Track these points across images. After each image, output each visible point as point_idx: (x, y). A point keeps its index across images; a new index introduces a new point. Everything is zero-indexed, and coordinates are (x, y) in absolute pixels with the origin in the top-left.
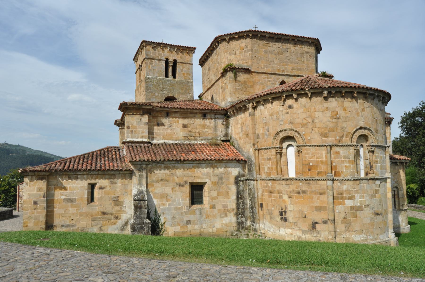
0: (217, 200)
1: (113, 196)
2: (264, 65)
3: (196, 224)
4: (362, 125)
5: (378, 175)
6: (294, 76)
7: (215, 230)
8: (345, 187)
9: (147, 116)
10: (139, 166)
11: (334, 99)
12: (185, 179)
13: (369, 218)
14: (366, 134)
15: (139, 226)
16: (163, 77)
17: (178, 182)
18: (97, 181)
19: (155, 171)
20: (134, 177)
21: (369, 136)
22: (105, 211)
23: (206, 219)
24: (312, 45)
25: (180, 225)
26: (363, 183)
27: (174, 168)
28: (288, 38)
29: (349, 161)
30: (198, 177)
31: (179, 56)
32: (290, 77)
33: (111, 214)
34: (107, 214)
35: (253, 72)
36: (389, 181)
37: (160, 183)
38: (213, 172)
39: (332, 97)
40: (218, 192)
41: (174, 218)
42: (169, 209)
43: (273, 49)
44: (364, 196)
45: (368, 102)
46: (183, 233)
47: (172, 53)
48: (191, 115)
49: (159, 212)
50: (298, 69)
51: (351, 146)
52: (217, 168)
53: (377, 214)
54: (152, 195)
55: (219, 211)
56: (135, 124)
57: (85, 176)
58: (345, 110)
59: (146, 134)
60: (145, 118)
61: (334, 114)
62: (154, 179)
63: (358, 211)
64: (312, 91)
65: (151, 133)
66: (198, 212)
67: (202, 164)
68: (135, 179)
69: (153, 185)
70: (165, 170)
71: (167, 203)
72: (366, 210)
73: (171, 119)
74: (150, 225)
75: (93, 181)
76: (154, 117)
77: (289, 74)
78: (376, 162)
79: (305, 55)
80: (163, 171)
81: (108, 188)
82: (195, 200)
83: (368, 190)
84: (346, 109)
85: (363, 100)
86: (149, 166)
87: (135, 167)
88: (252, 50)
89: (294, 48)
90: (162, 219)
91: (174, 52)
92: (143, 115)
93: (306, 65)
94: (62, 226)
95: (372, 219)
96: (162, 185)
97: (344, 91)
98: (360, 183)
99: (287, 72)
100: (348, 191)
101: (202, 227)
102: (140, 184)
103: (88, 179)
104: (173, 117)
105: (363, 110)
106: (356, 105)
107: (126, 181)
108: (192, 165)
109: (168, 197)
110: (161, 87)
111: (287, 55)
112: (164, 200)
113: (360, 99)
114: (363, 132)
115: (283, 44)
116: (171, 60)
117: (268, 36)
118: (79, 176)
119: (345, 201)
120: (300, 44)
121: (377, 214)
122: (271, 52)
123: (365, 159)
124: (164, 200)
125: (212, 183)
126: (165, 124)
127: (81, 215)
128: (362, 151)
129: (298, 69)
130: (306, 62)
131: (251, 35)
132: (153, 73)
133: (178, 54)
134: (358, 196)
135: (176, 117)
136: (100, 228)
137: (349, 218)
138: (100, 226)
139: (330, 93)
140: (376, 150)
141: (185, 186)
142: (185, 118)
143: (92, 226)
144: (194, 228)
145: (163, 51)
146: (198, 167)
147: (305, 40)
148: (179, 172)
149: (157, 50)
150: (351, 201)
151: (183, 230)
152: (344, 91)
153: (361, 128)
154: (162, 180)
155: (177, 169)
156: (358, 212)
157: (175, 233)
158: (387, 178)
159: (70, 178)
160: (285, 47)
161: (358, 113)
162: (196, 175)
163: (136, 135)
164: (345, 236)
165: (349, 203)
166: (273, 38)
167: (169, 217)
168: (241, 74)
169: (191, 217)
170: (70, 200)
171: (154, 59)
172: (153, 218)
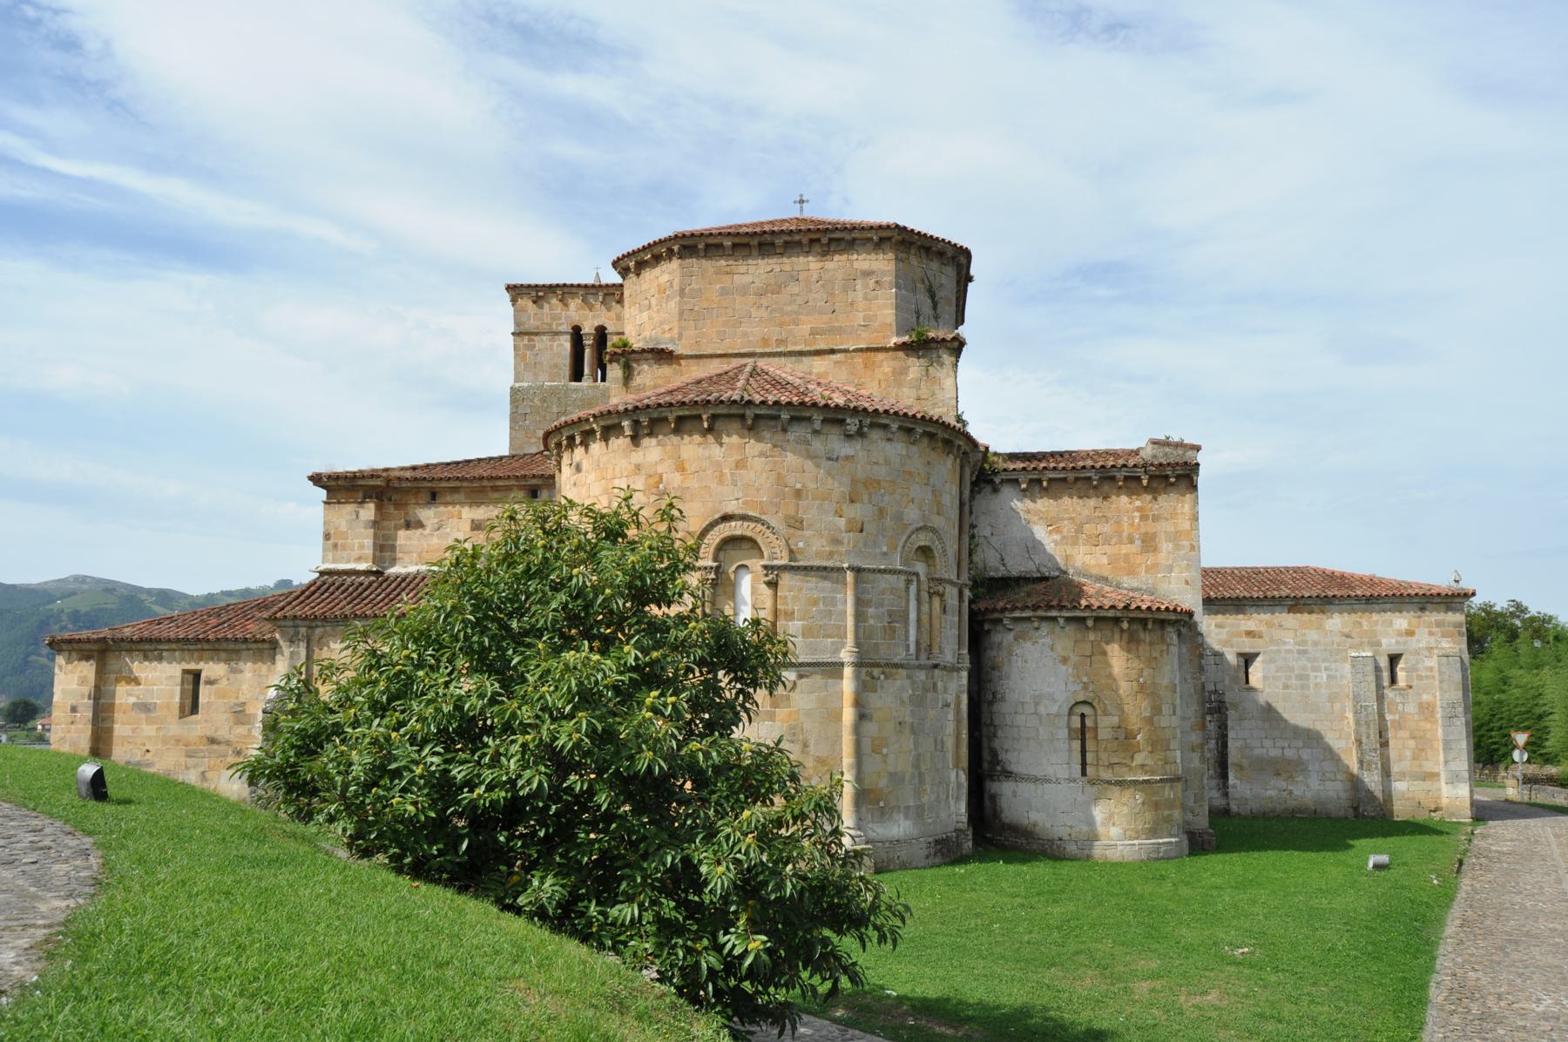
2: (718, 333)
4: (732, 507)
6: (818, 353)
9: (372, 506)
10: (291, 631)
11: (654, 441)
14: (749, 534)
16: (563, 380)
18: (201, 666)
20: (278, 657)
24: (886, 246)
28: (797, 238)
31: (612, 314)
32: (805, 359)
33: (228, 743)
34: (219, 743)
35: (681, 357)
36: (848, 671)
39: (650, 435)
43: (748, 279)
45: (759, 440)
47: (591, 308)
48: (496, 495)
50: (831, 331)
56: (343, 526)
58: (683, 470)
59: (369, 551)
60: (369, 511)
61: (652, 481)
64: (602, 423)
65: (384, 549)
73: (442, 509)
75: (192, 666)
76: (398, 505)
77: (798, 348)
78: (790, 615)
79: (858, 281)
81: (224, 682)
84: (687, 466)
85: (742, 437)
86: (318, 631)
87: (282, 635)
88: (682, 292)
89: (820, 265)
91: (598, 305)
92: (363, 502)
93: (861, 315)
97: (671, 417)
99: (795, 344)
104: (446, 504)
105: (740, 464)
106: (716, 451)
107: (263, 668)
110: (555, 410)
111: (796, 290)
113: (729, 435)
114: (735, 528)
115: (785, 260)
116: (588, 329)
117: (728, 243)
120: (840, 252)
122: (744, 290)
127: (165, 741)
129: (831, 331)
130: (861, 304)
131: (676, 248)
132: (535, 374)
133: (609, 310)
135: (453, 504)
139: (636, 424)
140: (786, 580)
142: (479, 504)
143: (187, 768)
145: (566, 305)
147: (856, 234)
149: (546, 306)
152: (671, 417)
153: (726, 518)
158: (842, 664)
159: (146, 658)
160: (787, 268)
161: (722, 475)
163: (345, 554)
166: (747, 245)
168: (646, 367)
170: (145, 708)
171: (537, 334)
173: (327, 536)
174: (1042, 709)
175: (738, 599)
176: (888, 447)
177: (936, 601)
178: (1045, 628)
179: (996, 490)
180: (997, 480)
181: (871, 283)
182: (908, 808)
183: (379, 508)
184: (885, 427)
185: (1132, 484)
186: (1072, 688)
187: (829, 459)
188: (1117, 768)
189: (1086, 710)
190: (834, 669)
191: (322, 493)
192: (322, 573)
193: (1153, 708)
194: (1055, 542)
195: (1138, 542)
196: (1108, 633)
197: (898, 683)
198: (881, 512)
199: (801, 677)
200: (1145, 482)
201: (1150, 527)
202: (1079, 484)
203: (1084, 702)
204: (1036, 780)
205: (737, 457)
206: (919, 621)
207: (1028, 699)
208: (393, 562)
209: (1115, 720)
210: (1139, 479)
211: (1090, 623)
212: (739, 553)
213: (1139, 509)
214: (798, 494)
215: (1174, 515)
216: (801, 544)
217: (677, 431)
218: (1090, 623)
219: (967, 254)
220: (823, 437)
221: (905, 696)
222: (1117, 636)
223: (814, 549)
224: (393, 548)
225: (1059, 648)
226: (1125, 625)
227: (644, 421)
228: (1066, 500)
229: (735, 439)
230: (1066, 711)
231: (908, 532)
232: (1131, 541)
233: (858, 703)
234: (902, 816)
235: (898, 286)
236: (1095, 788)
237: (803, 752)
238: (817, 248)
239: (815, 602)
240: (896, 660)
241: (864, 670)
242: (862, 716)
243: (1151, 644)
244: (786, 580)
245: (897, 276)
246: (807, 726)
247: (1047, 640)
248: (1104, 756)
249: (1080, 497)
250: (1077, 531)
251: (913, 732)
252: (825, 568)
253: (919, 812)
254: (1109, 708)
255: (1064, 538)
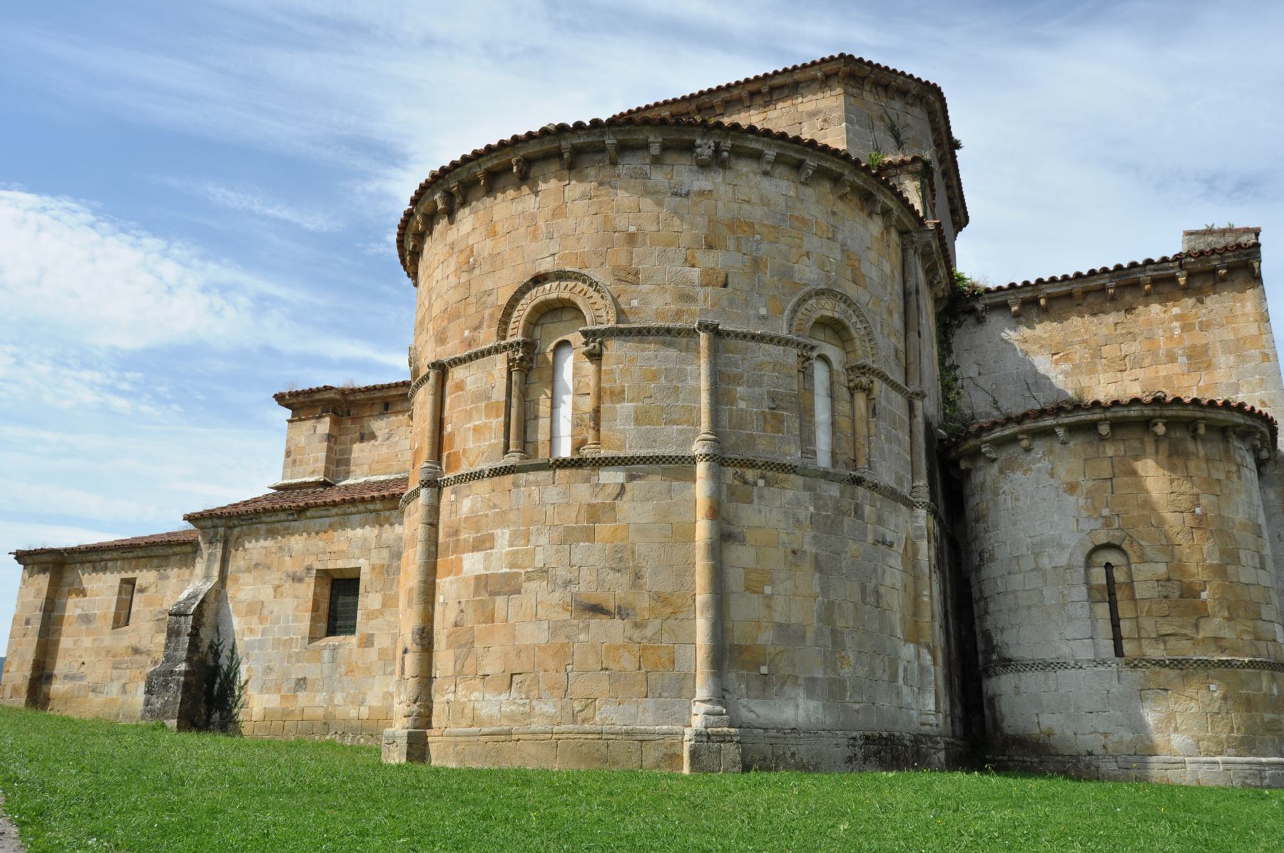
0: (380, 620)
1: (158, 608)
3: (318, 691)
4: (546, 266)
5: (622, 447)
7: (364, 713)
8: (466, 505)
9: (327, 420)
11: (467, 210)
12: (307, 563)
13: (545, 625)
14: (566, 295)
15: (162, 678)
17: (290, 570)
18: (137, 574)
19: (247, 545)
20: (198, 560)
21: (580, 302)
22: (138, 646)
23: (344, 678)
24: (834, 82)
25: (279, 690)
26: (528, 484)
27: (289, 532)
29: (486, 406)
30: (340, 554)
33: (148, 653)
36: (701, 468)
37: (255, 573)
38: (379, 537)
40: (384, 596)
41: (269, 669)
42: (261, 645)
44: (527, 536)
45: (581, 180)
46: (286, 713)
49: (240, 651)
51: (497, 350)
52: (392, 525)
53: (596, 610)
54: (231, 606)
55: (382, 652)
57: (119, 563)
58: (495, 234)
59: (321, 465)
60: (324, 425)
61: (462, 257)
62: (242, 563)
63: (498, 594)
65: (338, 461)
66: (326, 655)
67: (352, 517)
68: (200, 566)
69: (236, 581)
70: (266, 539)
71: (261, 627)
72: (535, 589)
73: (393, 418)
74: (182, 679)
75: (129, 575)
78: (618, 395)
79: (804, 124)
80: (262, 543)
81: (153, 589)
82: (339, 623)
83: (550, 509)
86: (236, 531)
87: (204, 537)
90: (243, 674)
92: (320, 417)
94: (66, 677)
95: (554, 629)
96: (255, 579)
98: (516, 485)
100: (474, 520)
101: (331, 699)
102: (207, 577)
103: (123, 569)
107: (185, 572)
108: (327, 520)
109: (265, 612)
112: (255, 619)
113: (545, 181)
114: (550, 291)
118: (110, 564)
119: (461, 560)
121: (596, 610)
123: (578, 393)
124: (255, 619)
125: (374, 569)
126: (377, 433)
128: (568, 366)
134: (503, 537)
136: (124, 685)
137: (470, 620)
138: (123, 681)
140: (614, 349)
141: (307, 580)
143: (112, 680)
144: (312, 703)
146: (343, 526)
148: (297, 542)
150: (479, 556)
151: (284, 706)
152: (479, 172)
153: (539, 280)
154: (257, 565)
155: (292, 534)
156: (500, 601)
157: (267, 714)
158: (693, 460)
159: (95, 570)
162: (335, 548)
163: (301, 469)
164: (451, 697)
165: (473, 564)
167: (258, 667)
169: (310, 670)
170: (87, 619)
172: (225, 668)
173: (288, 454)
174: (1045, 562)
175: (559, 387)
176: (766, 184)
177: (860, 399)
178: (1040, 447)
179: (980, 321)
180: (980, 306)
181: (819, 123)
182: (812, 681)
183: (336, 423)
184: (757, 156)
185: (1166, 288)
186: (1087, 526)
187: (676, 194)
188: (1172, 642)
189: (1113, 558)
190: (680, 466)
191: (288, 413)
192: (278, 488)
193: (1223, 552)
194: (1066, 374)
195: (1182, 360)
196: (1136, 444)
197: (790, 494)
198: (756, 263)
199: (631, 478)
200: (1182, 281)
201: (1199, 338)
202: (1090, 299)
203: (1109, 546)
204: (1045, 666)
205: (553, 205)
206: (833, 424)
207: (1024, 551)
208: (347, 475)
209: (1161, 569)
210: (1173, 279)
211: (1104, 429)
212: (560, 326)
213: (1177, 318)
214: (632, 239)
215: (1231, 318)
216: (635, 303)
217: (490, 191)
218: (1104, 429)
219: (935, 90)
220: (667, 169)
221: (803, 514)
222: (1150, 448)
223: (652, 305)
224: (347, 462)
225: (1062, 472)
226: (1161, 429)
227: (453, 185)
228: (1075, 321)
229: (553, 183)
230: (1080, 559)
231: (801, 294)
232: (1172, 358)
233: (716, 512)
234: (801, 693)
235: (848, 120)
236: (1138, 674)
237: (634, 585)
238: (758, 100)
239: (655, 377)
240: (788, 460)
241: (730, 471)
242: (724, 537)
243: (1208, 459)
244: (614, 349)
245: (846, 110)
246: (641, 548)
247: (1045, 464)
248: (1148, 625)
249: (1094, 314)
250: (1093, 356)
251: (818, 565)
252: (669, 331)
253: (834, 691)
254: (1149, 552)
255: (1076, 366)
